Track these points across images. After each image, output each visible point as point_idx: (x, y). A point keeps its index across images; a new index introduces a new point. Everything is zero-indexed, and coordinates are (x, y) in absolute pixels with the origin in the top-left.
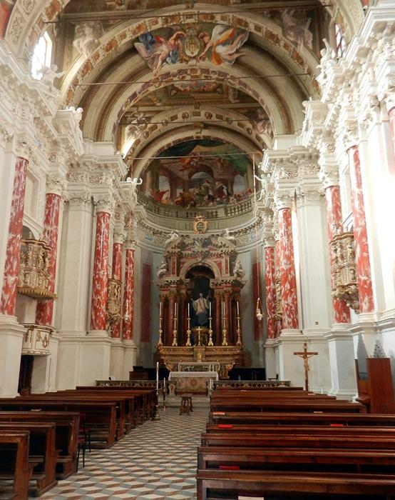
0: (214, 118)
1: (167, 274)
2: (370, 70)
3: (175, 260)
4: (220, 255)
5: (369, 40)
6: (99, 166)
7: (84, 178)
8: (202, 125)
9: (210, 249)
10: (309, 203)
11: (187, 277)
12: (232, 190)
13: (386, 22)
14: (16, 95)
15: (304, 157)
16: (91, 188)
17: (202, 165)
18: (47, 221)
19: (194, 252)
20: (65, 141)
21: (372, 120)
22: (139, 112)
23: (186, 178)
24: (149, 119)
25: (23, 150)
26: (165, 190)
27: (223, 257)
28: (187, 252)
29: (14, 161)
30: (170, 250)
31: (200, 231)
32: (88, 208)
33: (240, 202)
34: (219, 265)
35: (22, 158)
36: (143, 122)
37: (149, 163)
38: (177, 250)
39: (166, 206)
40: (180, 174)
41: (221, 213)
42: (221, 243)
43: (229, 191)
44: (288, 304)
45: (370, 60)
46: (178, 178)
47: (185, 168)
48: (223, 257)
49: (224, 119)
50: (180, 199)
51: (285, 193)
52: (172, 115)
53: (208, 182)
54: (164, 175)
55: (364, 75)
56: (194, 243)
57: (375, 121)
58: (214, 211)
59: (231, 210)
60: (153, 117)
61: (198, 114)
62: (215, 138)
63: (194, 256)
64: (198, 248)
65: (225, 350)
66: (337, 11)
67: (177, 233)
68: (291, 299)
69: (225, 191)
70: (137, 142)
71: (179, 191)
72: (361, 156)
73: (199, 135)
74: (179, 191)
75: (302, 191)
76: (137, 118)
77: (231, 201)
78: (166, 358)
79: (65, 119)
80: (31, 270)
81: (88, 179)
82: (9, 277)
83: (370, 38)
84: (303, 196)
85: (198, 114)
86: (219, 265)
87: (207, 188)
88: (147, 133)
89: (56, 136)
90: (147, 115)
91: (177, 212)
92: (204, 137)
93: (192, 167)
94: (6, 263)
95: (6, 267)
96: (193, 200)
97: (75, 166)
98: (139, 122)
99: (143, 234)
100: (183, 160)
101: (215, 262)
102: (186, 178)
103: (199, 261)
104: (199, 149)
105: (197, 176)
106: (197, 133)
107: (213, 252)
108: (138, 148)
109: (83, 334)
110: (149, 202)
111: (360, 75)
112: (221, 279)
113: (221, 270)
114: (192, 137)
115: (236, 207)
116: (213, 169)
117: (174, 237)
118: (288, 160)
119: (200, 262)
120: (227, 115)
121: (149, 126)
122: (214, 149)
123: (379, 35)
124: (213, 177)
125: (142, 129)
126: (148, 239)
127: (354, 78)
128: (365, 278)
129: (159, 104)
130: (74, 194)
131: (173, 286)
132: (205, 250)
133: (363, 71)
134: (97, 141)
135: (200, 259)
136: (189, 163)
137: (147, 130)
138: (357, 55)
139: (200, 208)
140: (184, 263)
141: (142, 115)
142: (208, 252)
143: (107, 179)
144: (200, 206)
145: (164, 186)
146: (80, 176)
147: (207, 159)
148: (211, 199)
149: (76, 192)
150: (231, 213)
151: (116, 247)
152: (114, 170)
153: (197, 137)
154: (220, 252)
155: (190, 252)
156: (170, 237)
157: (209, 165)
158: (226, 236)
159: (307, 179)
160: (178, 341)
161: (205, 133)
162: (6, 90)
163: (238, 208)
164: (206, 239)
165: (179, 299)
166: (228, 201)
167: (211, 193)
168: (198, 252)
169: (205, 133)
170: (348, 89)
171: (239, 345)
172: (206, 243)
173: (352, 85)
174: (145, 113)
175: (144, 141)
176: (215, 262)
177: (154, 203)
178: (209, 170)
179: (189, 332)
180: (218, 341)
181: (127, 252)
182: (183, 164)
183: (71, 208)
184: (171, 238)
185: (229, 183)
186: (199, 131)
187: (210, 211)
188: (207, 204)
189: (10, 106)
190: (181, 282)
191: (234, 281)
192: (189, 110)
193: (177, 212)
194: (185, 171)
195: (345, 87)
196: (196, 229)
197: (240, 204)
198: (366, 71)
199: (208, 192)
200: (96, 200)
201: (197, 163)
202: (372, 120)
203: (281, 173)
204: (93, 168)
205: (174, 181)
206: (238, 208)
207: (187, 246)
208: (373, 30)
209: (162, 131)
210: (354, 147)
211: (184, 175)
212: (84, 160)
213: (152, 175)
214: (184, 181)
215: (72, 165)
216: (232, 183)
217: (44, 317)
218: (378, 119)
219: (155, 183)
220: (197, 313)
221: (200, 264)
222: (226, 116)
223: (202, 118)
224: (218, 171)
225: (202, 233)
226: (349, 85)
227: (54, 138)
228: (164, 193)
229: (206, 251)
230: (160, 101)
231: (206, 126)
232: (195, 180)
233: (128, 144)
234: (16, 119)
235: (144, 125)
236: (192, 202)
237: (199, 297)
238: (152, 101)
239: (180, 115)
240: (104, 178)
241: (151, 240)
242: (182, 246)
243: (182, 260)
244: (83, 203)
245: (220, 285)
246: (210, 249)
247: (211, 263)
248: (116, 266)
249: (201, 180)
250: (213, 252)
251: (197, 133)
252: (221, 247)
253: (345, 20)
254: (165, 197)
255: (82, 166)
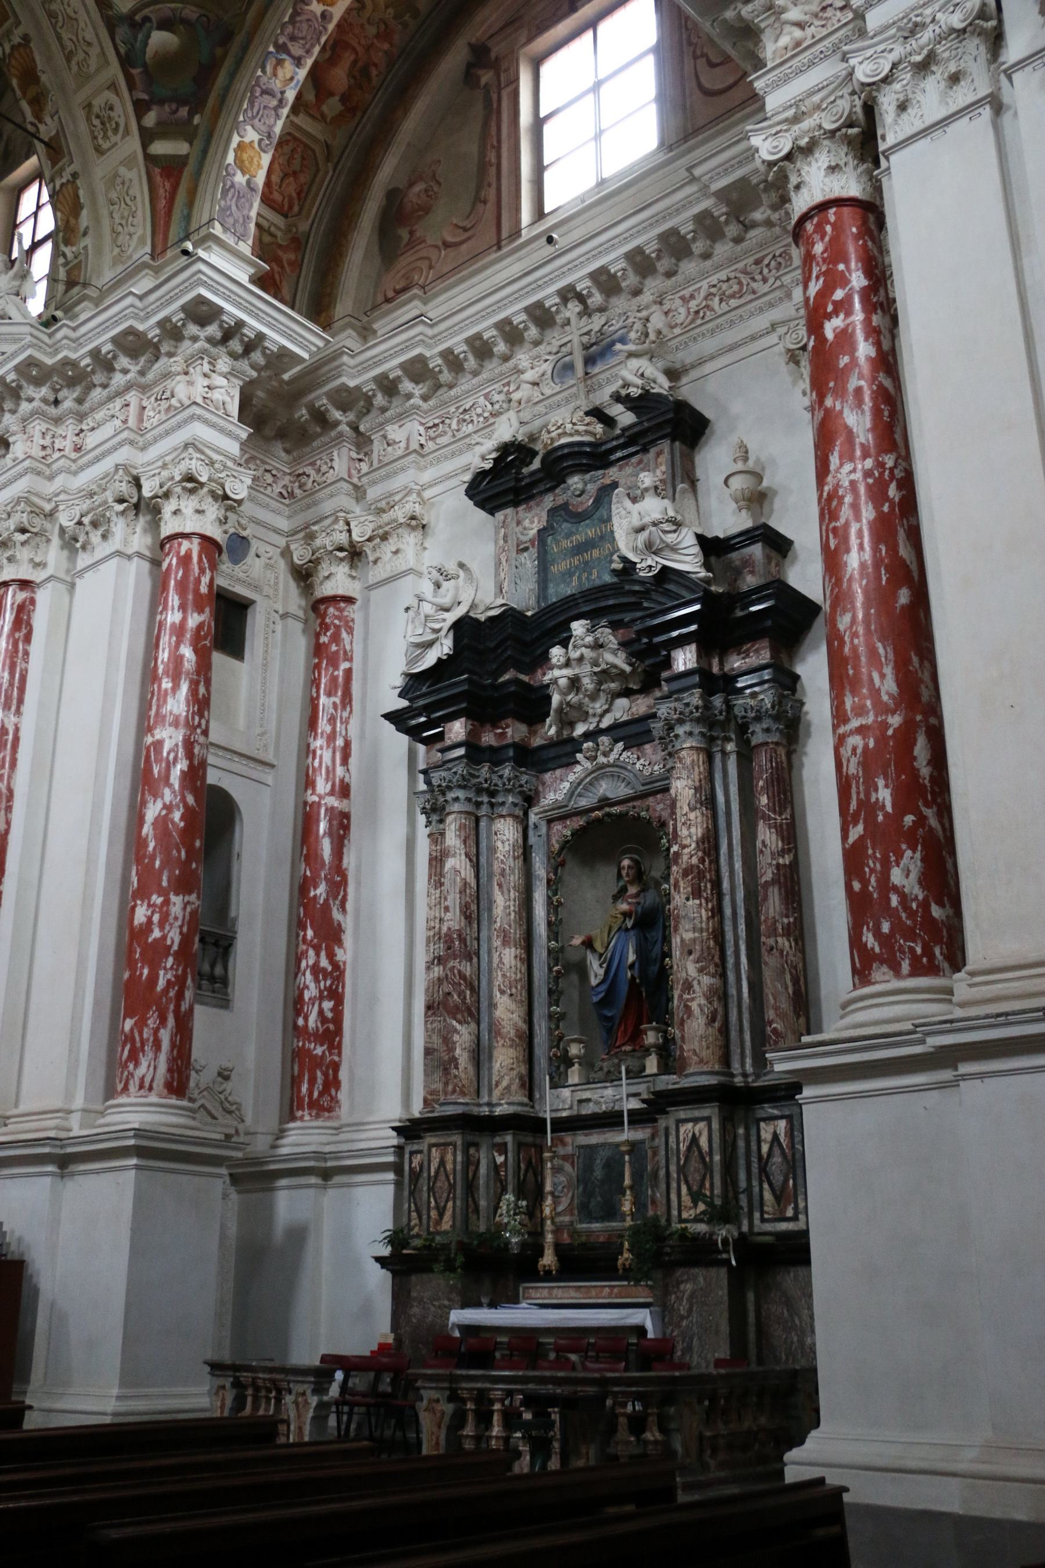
2: (132, 397)
5: (161, 324)
13: (220, 310)
21: (104, 537)
45: (142, 373)
55: (110, 399)
57: (116, 543)
66: (66, 177)
72: (40, 620)
83: (167, 319)
111: (97, 394)
123: (193, 329)
127: (77, 392)
133: (112, 389)
138: (114, 340)
170: (53, 411)
173: (68, 404)
195: (44, 400)
198: (118, 394)
202: (104, 537)
208: (184, 308)
210: (25, 584)
218: (126, 542)
226: (56, 402)
253: (84, 213)
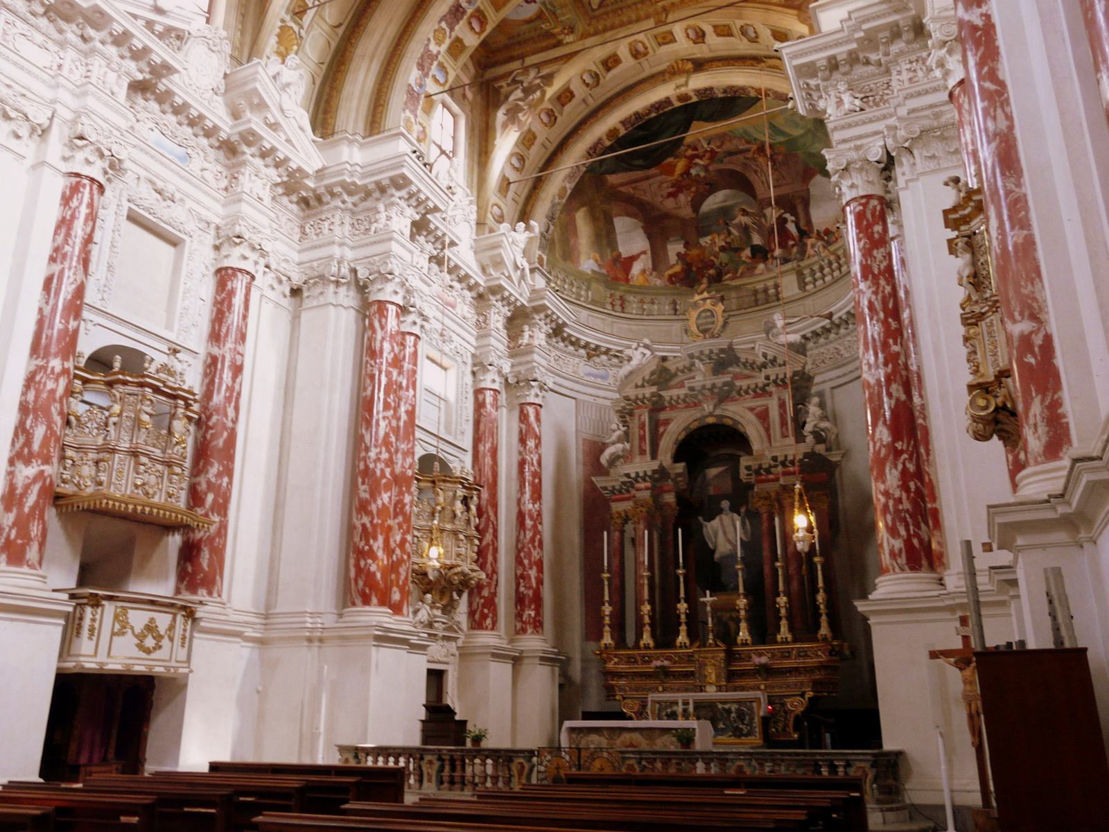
0: (711, 38)
1: (626, 457)
3: (646, 418)
4: (763, 389)
6: (368, 194)
7: (337, 230)
8: (690, 66)
9: (736, 377)
10: (932, 165)
11: (677, 458)
12: (809, 222)
14: (61, 31)
15: (896, 33)
16: (353, 248)
17: (720, 172)
18: (216, 336)
19: (692, 389)
20: (250, 138)
22: (526, 70)
23: (687, 212)
24: (548, 79)
25: (80, 156)
26: (635, 253)
27: (770, 394)
28: (674, 393)
29: (56, 185)
30: (632, 392)
31: (704, 332)
32: (348, 297)
33: (832, 248)
34: (763, 416)
35: (78, 175)
36: (539, 87)
37: (569, 187)
38: (648, 391)
39: (641, 291)
40: (669, 204)
41: (789, 285)
42: (765, 355)
43: (802, 223)
44: (886, 494)
46: (667, 216)
47: (678, 188)
48: (770, 394)
49: (736, 31)
50: (678, 268)
51: (853, 155)
52: (601, 53)
53: (745, 213)
54: (628, 215)
56: (690, 368)
58: (770, 283)
59: (813, 273)
60: (558, 70)
61: (669, 39)
62: (725, 91)
63: (691, 402)
64: (702, 377)
65: (786, 655)
67: (646, 347)
68: (896, 473)
69: (791, 227)
70: (528, 139)
71: (675, 249)
73: (683, 90)
74: (675, 249)
75: (902, 133)
76: (522, 82)
77: (810, 251)
78: (622, 682)
79: (250, 86)
80: (113, 451)
81: (347, 227)
82: (20, 466)
84: (909, 151)
85: (669, 39)
86: (763, 416)
87: (745, 229)
88: (550, 113)
89: (227, 128)
90: (545, 71)
91: (674, 303)
92: (698, 92)
93: (697, 180)
94: (16, 435)
95: (13, 444)
96: (712, 265)
97: (313, 202)
98: (527, 91)
99: (577, 365)
100: (670, 170)
101: (751, 409)
102: (687, 212)
103: (708, 411)
104: (700, 132)
105: (713, 202)
106: (678, 87)
107: (743, 383)
108: (536, 154)
109: (329, 621)
110: (594, 285)
112: (769, 455)
113: (767, 430)
114: (667, 101)
115: (825, 264)
116: (752, 177)
117: (639, 357)
118: (853, 59)
119: (711, 415)
120: (740, 17)
121: (551, 91)
122: (736, 123)
124: (754, 195)
125: (532, 106)
126: (596, 376)
128: (1024, 326)
129: (569, 39)
130: (312, 268)
131: (642, 485)
132: (720, 380)
134: (371, 135)
135: (708, 407)
136: (686, 173)
137: (546, 105)
139: (734, 283)
140: (667, 422)
141: (533, 74)
142: (729, 384)
143: (389, 218)
144: (732, 279)
145: (631, 239)
146: (326, 224)
147: (730, 154)
148: (761, 254)
149: (315, 264)
150: (815, 280)
151: (481, 397)
152: (404, 193)
153: (680, 98)
154: (760, 379)
155: (682, 392)
156: (630, 359)
157: (738, 169)
158: (778, 335)
159: (919, 94)
160: (689, 635)
161: (699, 81)
162: (25, 21)
163: (830, 264)
164: (722, 351)
165: (659, 523)
166: (803, 252)
167: (757, 240)
168: (704, 387)
169: (699, 81)
171: (825, 639)
172: (724, 361)
174: (538, 66)
175: (547, 136)
176: (751, 409)
177: (607, 287)
178: (742, 183)
179: (683, 607)
180: (763, 631)
181: (522, 411)
182: (671, 178)
183: (307, 303)
184: (634, 362)
185: (796, 203)
186: (682, 80)
187: (760, 286)
188: (751, 270)
189: (44, 59)
190: (662, 473)
191: (806, 455)
192: (643, 34)
193: (674, 303)
194: (682, 197)
196: (694, 329)
197: (834, 253)
199: (749, 238)
200: (362, 274)
201: (706, 168)
203: (840, 102)
204: (356, 198)
205: (658, 227)
206: (830, 264)
207: (675, 375)
209: (593, 104)
211: (682, 206)
212: (327, 182)
213: (593, 218)
214: (683, 221)
215: (305, 202)
216: (806, 202)
217: (193, 576)
219: (605, 237)
220: (717, 556)
221: (711, 420)
222: (739, 23)
223: (683, 46)
224: (769, 184)
225: (713, 337)
227: (223, 136)
228: (633, 259)
229: (725, 384)
230: (572, 30)
231: (700, 65)
232: (707, 216)
233: (505, 143)
234: (57, 86)
235: (538, 93)
236: (712, 272)
237: (720, 511)
238: (553, 35)
239: (623, 50)
240: (383, 216)
241: (603, 378)
242: (662, 375)
243: (663, 416)
244: (332, 288)
245: (768, 471)
246: (736, 377)
247: (740, 413)
248: (481, 448)
249: (725, 214)
250: (743, 383)
251: (678, 87)
252: (764, 366)
254: (637, 268)
255: (327, 198)
